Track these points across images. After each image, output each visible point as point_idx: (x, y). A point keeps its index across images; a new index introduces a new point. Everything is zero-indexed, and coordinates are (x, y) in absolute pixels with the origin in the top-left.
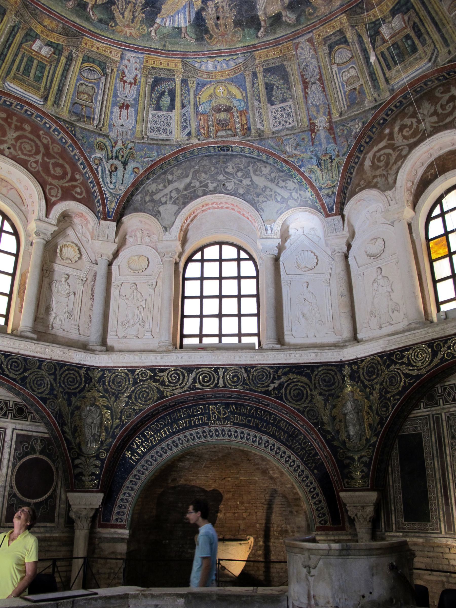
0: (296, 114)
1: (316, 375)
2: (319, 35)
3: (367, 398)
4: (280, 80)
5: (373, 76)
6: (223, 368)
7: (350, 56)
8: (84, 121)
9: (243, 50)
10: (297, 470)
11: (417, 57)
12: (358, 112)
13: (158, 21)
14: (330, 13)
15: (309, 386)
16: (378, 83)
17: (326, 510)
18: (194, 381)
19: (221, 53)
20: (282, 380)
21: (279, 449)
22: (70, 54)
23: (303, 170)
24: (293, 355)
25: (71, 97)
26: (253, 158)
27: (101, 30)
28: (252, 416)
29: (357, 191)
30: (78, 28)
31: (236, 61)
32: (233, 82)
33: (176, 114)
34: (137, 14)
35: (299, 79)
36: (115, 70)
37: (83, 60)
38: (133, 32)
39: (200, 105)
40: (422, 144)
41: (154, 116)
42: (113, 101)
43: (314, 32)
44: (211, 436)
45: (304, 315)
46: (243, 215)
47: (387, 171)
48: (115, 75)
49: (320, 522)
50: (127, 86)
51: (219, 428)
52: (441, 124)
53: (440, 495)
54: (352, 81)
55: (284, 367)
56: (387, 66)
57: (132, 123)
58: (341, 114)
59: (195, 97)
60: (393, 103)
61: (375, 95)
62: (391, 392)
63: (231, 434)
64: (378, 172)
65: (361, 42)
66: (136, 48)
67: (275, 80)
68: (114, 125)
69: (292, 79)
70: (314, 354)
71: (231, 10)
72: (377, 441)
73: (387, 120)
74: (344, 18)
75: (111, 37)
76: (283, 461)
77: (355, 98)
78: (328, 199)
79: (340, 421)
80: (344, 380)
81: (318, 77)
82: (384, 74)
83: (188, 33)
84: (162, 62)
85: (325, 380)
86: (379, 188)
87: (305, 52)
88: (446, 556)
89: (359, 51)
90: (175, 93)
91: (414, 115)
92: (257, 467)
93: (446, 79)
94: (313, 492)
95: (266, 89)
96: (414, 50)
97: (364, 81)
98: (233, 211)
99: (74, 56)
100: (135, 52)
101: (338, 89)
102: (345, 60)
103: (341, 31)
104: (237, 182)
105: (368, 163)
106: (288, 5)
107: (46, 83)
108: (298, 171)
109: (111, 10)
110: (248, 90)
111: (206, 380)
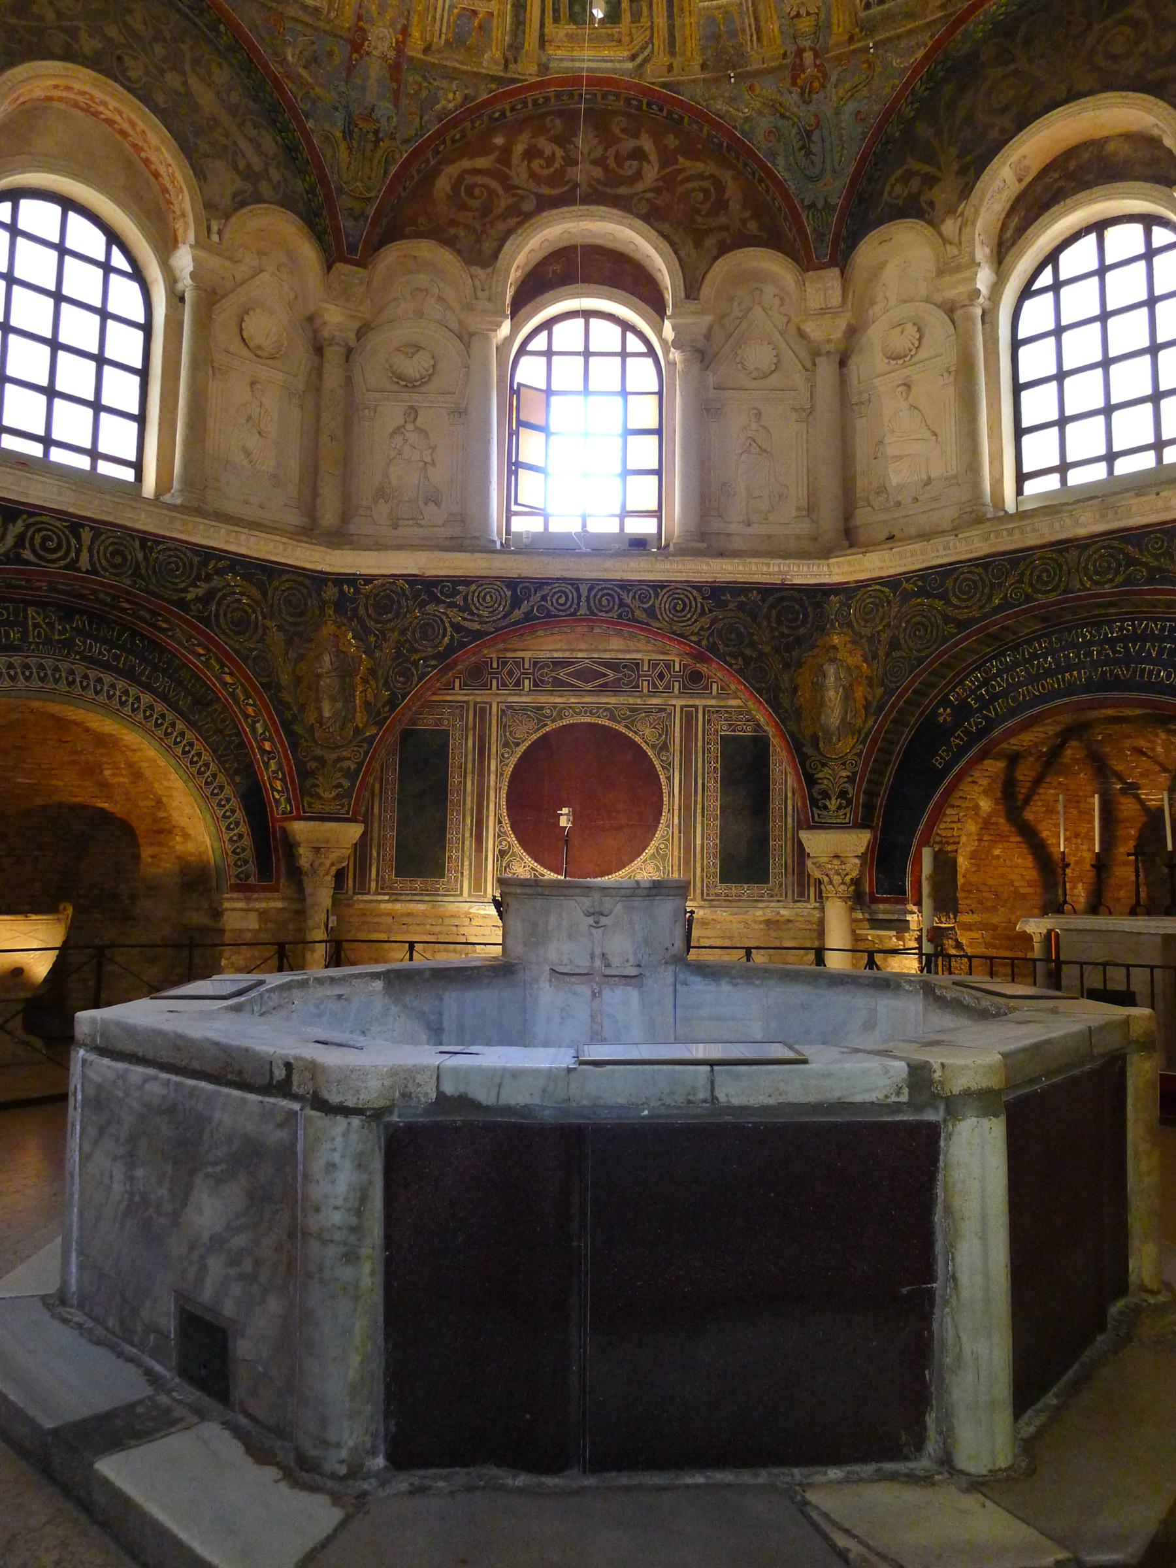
1: (276, 589)
3: (369, 653)
6: (92, 528)
10: (204, 773)
11: (612, 35)
15: (262, 609)
17: (249, 854)
18: (20, 539)
20: (212, 584)
21: (173, 725)
23: (310, 125)
24: (243, 537)
26: (195, 24)
28: (122, 648)
29: (407, 230)
40: (566, 209)
44: (27, 679)
45: (248, 454)
46: (146, 162)
47: (484, 225)
49: (237, 876)
51: (48, 663)
52: (609, 190)
53: (467, 835)
55: (221, 558)
56: (554, 10)
58: (427, 50)
62: (419, 651)
63: (74, 682)
64: (461, 217)
70: (281, 547)
72: (377, 734)
73: (505, 117)
76: (179, 751)
78: (350, 223)
79: (309, 688)
80: (322, 609)
82: (542, 25)
85: (290, 601)
86: (459, 252)
88: (462, 931)
91: (562, 140)
92: (75, 757)
93: (639, 108)
94: (229, 817)
98: (119, 137)
104: (153, 70)
105: (442, 185)
108: (300, 122)
111: (51, 545)
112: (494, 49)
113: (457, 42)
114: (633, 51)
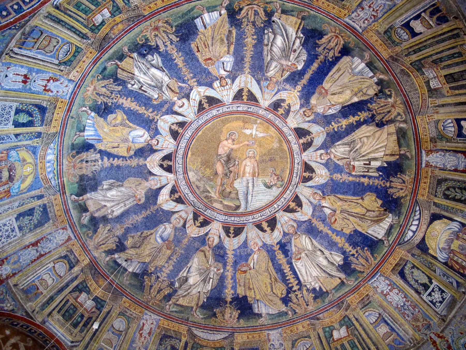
0: (9, 244)
2: (73, 245)
4: (38, 220)
5: (51, 301)
7: (61, 275)
8: (21, 39)
9: (62, 184)
12: (21, 300)
13: (93, 114)
14: (89, 250)
16: (47, 307)
19: (60, 165)
22: (87, 38)
25: (50, 31)
27: (98, 67)
30: (106, 49)
31: (53, 179)
32: (36, 178)
33: (10, 129)
34: (102, 97)
35: (39, 237)
36: (61, 74)
37: (79, 47)
38: (89, 93)
39: (17, 151)
41: (11, 107)
42: (34, 69)
43: (76, 240)
48: (56, 73)
50: (45, 83)
54: (44, 284)
57: (7, 85)
58: (15, 285)
59: (24, 146)
60: (34, 328)
61: (37, 309)
65: (72, 280)
66: (75, 93)
67: (37, 215)
68: (8, 68)
69: (38, 230)
71: (92, 172)
74: (87, 261)
75: (90, 74)
77: (31, 292)
81: (42, 253)
82: (54, 309)
83: (79, 138)
84: (59, 115)
87: (61, 236)
89: (66, 281)
90: (30, 127)
95: (30, 210)
96: (75, 325)
97: (46, 294)
99: (85, 41)
100: (72, 92)
101: (35, 274)
102: (58, 272)
103: (78, 261)
106: (94, 217)
107: (71, 11)
109: (110, 78)
110: (28, 194)
112: (34, 303)
113: (26, 292)
114: (73, 340)
